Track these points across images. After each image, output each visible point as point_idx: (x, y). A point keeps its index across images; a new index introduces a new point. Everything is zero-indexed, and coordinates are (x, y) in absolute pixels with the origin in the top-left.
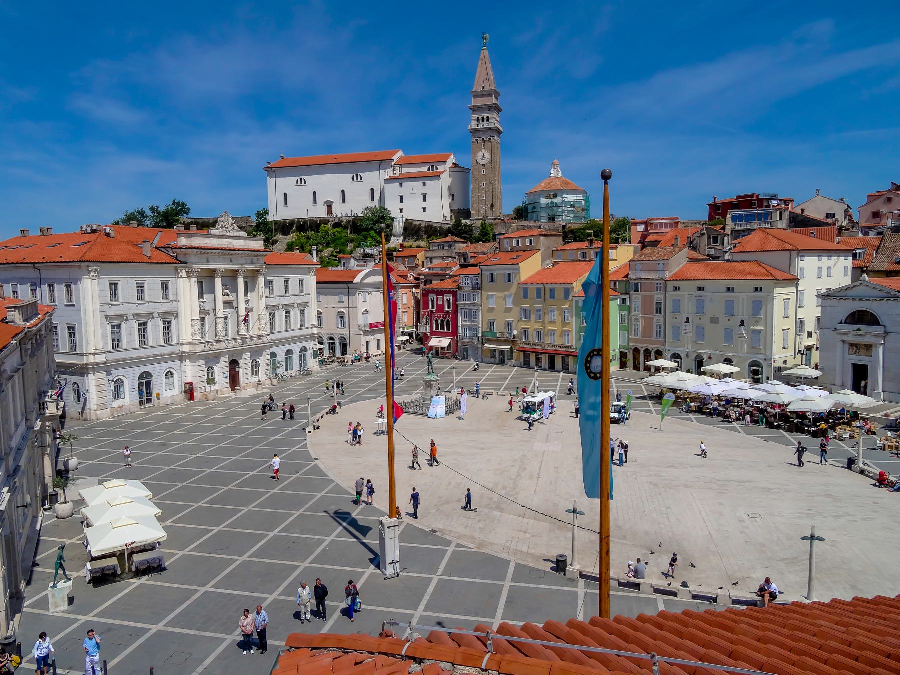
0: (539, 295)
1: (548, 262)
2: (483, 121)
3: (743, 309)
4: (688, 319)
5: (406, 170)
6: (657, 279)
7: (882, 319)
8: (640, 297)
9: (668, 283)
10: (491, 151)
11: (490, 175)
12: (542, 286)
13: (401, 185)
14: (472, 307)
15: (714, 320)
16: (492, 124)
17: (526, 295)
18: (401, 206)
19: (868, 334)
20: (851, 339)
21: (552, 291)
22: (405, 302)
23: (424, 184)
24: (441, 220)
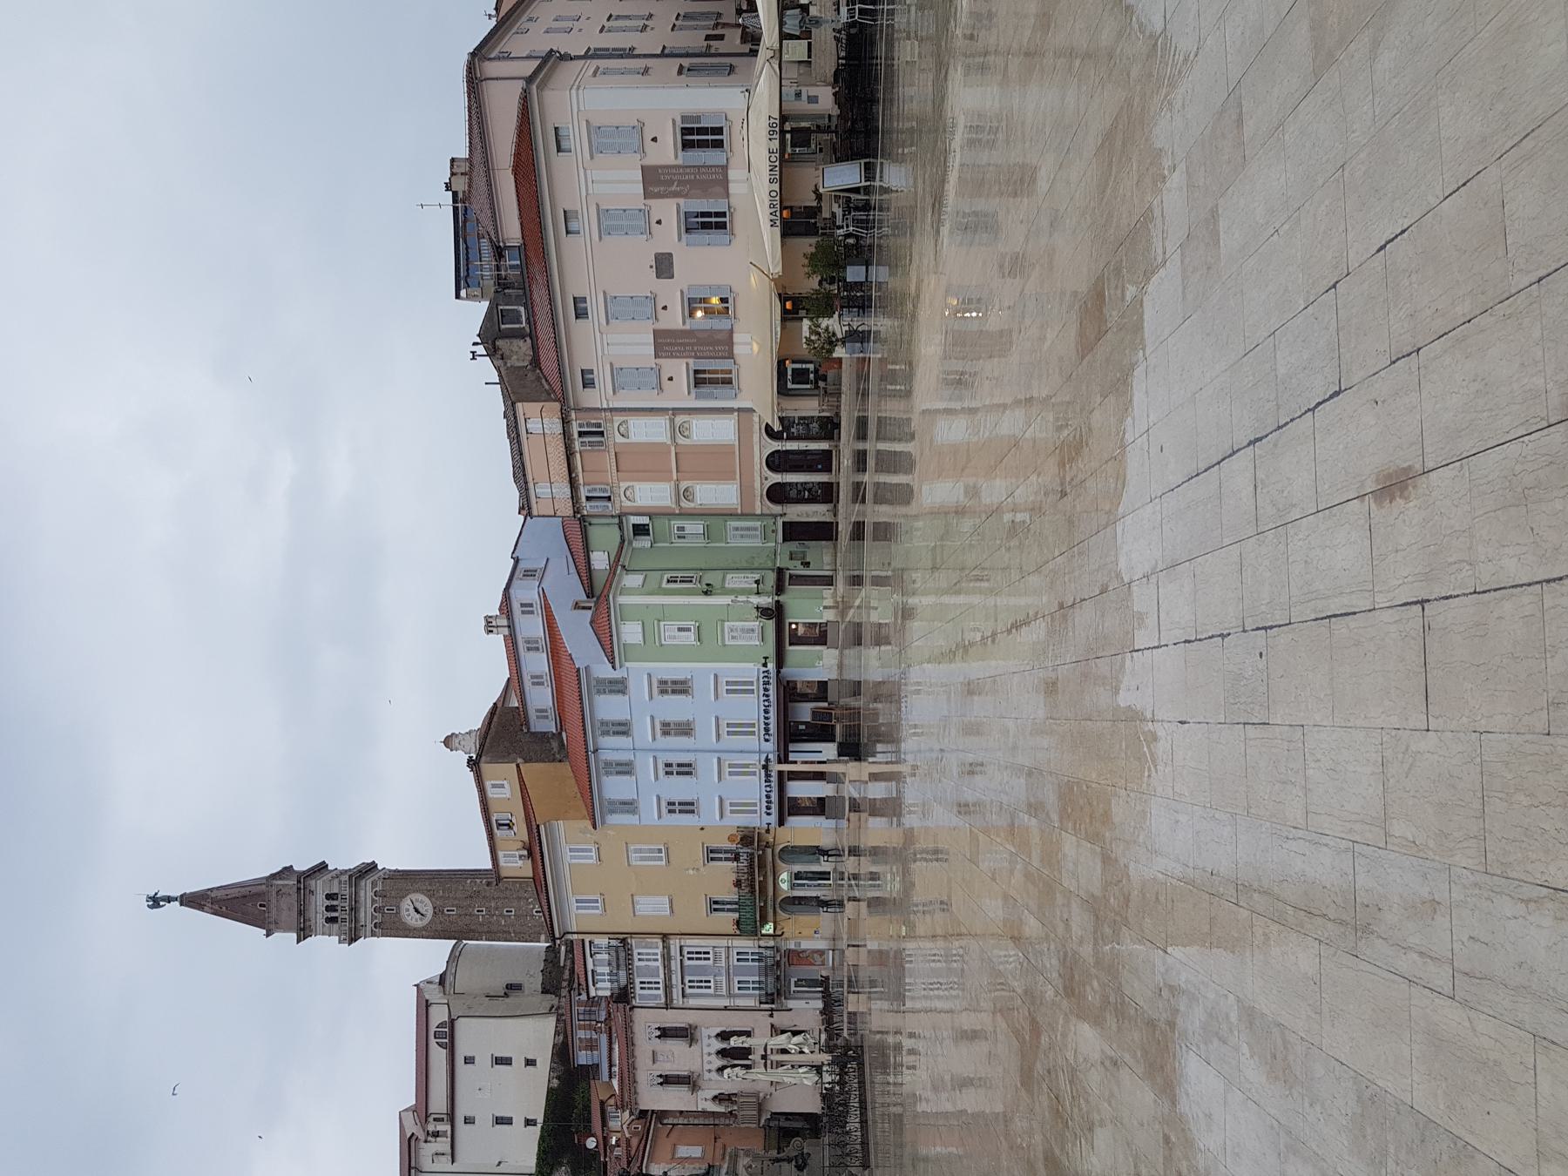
0: (625, 769)
5: (438, 1103)
6: (566, 434)
8: (624, 485)
13: (469, 1121)
18: (519, 1121)
22: (696, 1152)
23: (469, 1060)
24: (552, 1020)
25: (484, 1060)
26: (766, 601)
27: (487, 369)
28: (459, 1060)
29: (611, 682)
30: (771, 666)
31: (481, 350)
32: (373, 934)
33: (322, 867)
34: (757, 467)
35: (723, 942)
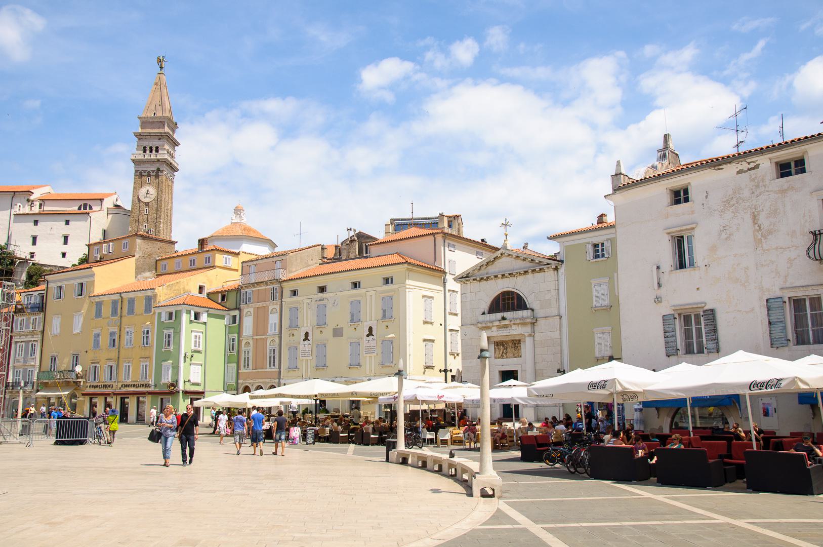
0: (114, 312)
1: (148, 274)
2: (151, 151)
3: (371, 315)
4: (307, 334)
6: (271, 282)
7: (530, 301)
8: (252, 310)
9: (284, 284)
10: (158, 187)
11: (154, 216)
12: (117, 297)
14: (29, 338)
15: (338, 332)
16: (163, 155)
17: (98, 314)
18: (33, 249)
19: (513, 325)
20: (496, 333)
21: (132, 302)
23: (67, 222)
25: (66, 230)
26: (181, 387)
27: (345, 236)
28: (67, 217)
29: (150, 305)
30: (152, 389)
31: (352, 233)
32: (136, 172)
33: (175, 144)
34: (257, 381)
35: (38, 364)
